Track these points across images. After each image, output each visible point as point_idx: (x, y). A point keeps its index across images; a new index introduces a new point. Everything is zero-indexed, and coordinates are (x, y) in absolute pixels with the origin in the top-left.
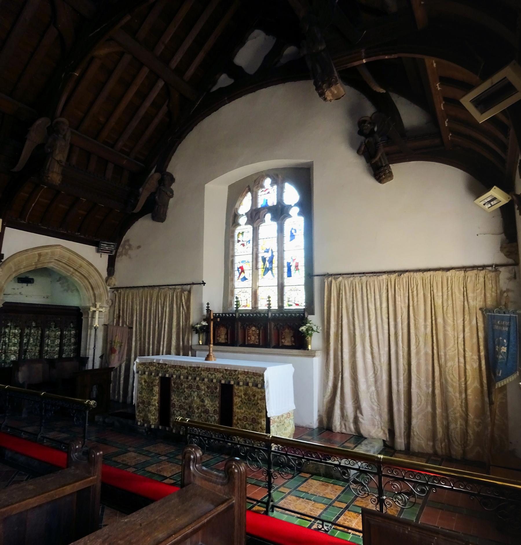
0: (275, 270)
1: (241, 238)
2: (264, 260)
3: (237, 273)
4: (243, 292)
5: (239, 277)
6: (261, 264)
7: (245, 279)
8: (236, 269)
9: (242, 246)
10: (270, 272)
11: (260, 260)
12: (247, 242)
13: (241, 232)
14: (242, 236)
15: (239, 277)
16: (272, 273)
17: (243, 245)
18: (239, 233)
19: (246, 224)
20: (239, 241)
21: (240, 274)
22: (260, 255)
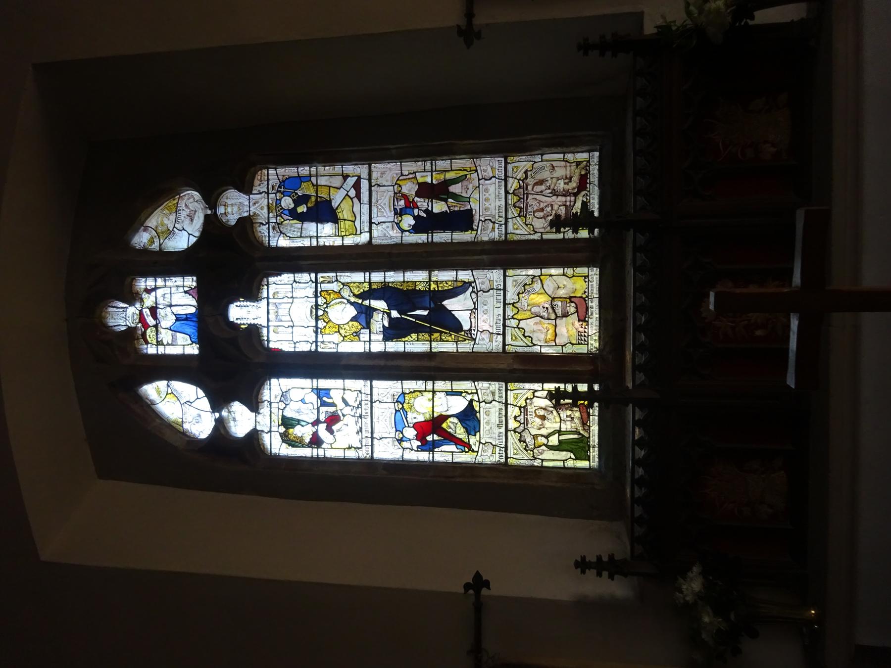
0: (445, 277)
1: (304, 432)
2: (394, 331)
3: (446, 454)
4: (526, 422)
5: (458, 442)
6: (415, 345)
7: (469, 417)
8: (424, 456)
9: (335, 428)
10: (449, 304)
11: (394, 346)
12: (324, 404)
13: (282, 429)
14: (298, 428)
15: (458, 442)
16: (456, 291)
17: (333, 420)
18: (286, 438)
19: (254, 405)
20: (316, 441)
21: (450, 438)
22: (378, 347)
